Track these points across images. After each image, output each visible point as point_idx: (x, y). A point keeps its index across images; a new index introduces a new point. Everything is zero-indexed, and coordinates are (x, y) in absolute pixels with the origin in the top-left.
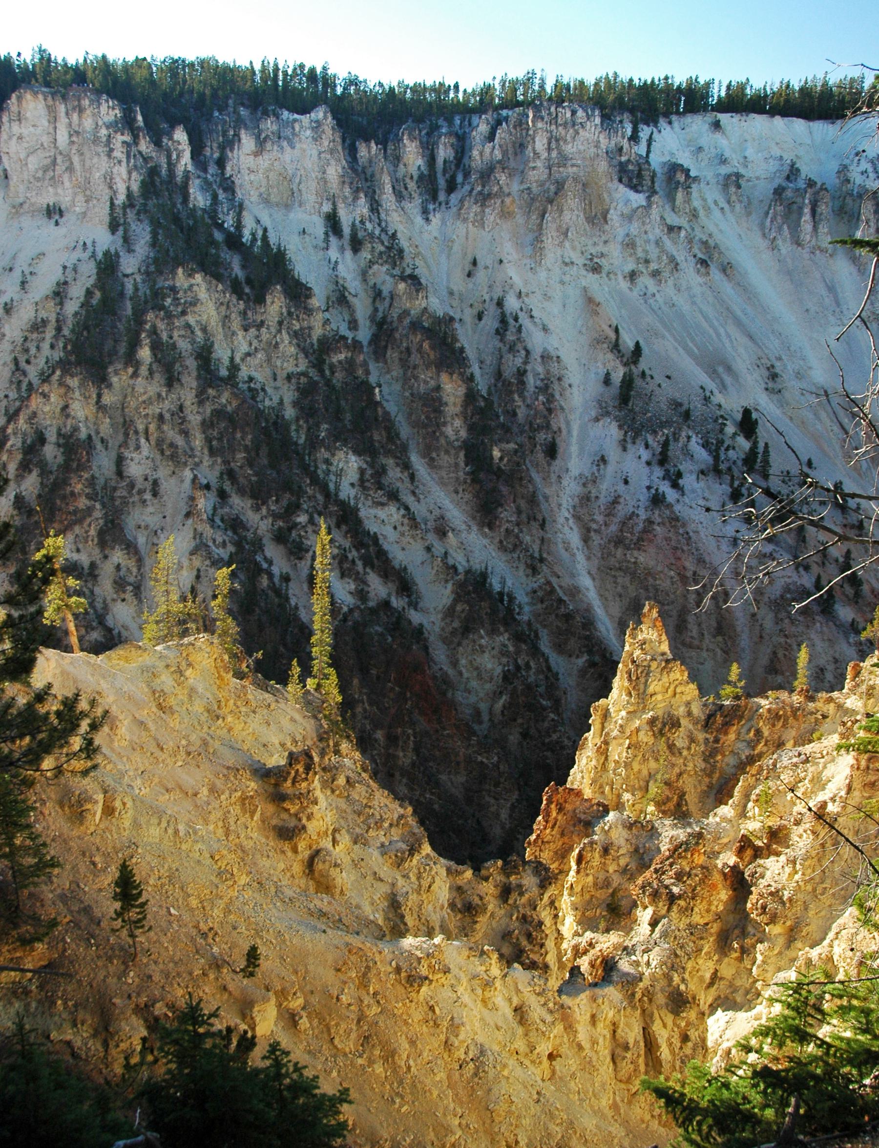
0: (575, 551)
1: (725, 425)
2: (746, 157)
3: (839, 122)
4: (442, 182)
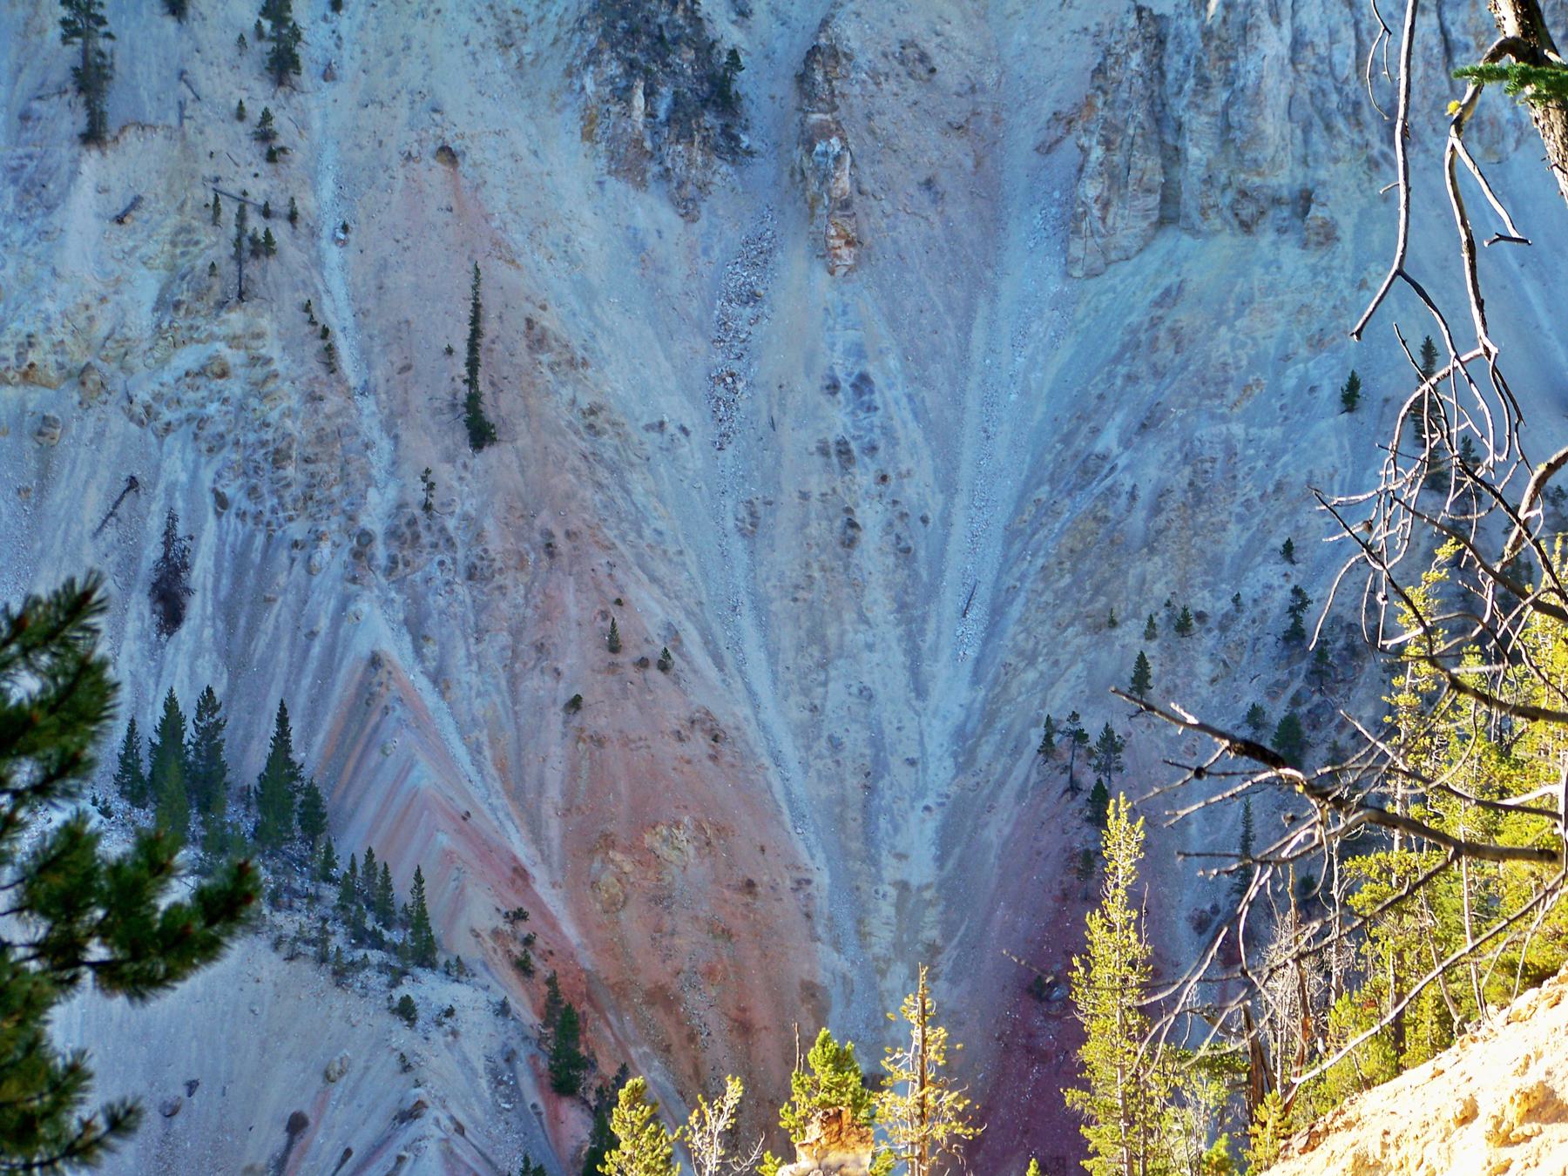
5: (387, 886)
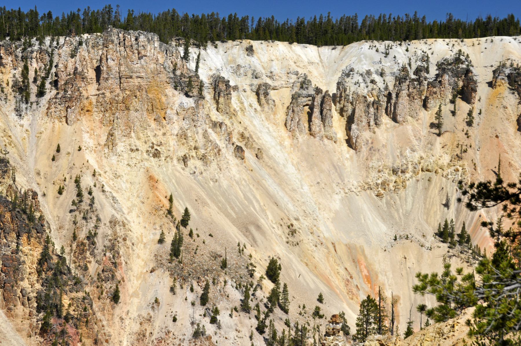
1: (254, 270)
2: (271, 72)
3: (339, 48)
4: (34, 89)
5: (480, 251)
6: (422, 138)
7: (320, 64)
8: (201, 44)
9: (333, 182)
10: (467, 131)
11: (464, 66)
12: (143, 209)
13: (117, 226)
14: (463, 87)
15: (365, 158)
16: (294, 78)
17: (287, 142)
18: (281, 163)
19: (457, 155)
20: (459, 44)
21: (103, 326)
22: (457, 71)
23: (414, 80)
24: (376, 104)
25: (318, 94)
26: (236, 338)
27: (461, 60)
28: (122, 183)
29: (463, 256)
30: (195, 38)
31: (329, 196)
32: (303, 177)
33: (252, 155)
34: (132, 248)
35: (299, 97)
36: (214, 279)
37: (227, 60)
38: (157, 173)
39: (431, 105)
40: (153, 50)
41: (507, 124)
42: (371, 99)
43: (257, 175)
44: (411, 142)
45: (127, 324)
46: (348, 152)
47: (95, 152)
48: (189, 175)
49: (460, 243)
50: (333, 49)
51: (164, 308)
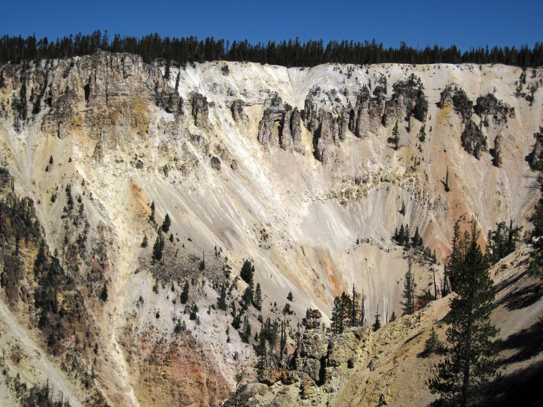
0: (122, 369)
1: (229, 272)
2: (245, 90)
3: (307, 69)
4: (30, 106)
5: (430, 252)
6: (381, 152)
7: (290, 83)
8: (181, 64)
9: (301, 190)
10: (420, 146)
11: (417, 88)
12: (128, 215)
13: (104, 231)
14: (416, 106)
15: (330, 169)
16: (265, 96)
17: (260, 154)
18: (254, 173)
19: (411, 167)
20: (412, 69)
21: (93, 321)
22: (411, 92)
23: (373, 99)
24: (340, 120)
25: (287, 111)
26: (214, 332)
27: (414, 82)
28: (108, 192)
29: (416, 257)
30: (175, 59)
31: (298, 204)
32: (275, 186)
33: (227, 165)
34: (118, 252)
35: (270, 113)
36: (193, 280)
37: (205, 79)
38: (140, 182)
39: (389, 122)
40: (137, 70)
41: (453, 140)
42: (335, 116)
43: (232, 184)
44: (371, 155)
45: (115, 320)
46: (315, 163)
47: (84, 163)
48: (170, 184)
49: (414, 245)
50: (301, 70)
51: (147, 305)
